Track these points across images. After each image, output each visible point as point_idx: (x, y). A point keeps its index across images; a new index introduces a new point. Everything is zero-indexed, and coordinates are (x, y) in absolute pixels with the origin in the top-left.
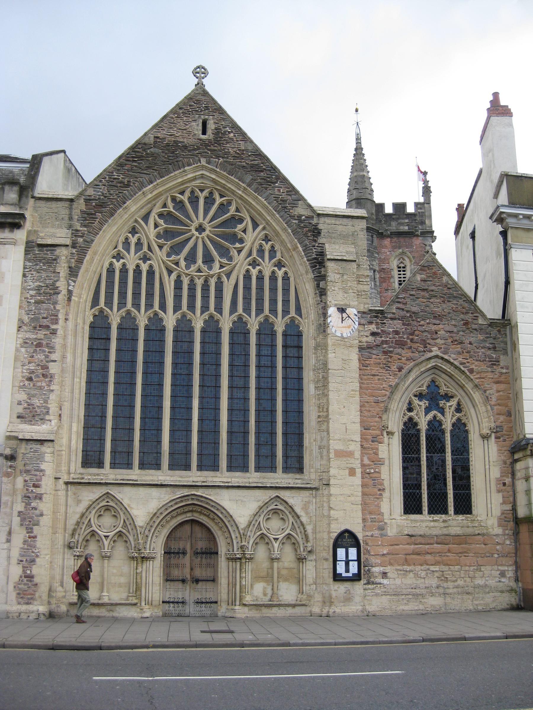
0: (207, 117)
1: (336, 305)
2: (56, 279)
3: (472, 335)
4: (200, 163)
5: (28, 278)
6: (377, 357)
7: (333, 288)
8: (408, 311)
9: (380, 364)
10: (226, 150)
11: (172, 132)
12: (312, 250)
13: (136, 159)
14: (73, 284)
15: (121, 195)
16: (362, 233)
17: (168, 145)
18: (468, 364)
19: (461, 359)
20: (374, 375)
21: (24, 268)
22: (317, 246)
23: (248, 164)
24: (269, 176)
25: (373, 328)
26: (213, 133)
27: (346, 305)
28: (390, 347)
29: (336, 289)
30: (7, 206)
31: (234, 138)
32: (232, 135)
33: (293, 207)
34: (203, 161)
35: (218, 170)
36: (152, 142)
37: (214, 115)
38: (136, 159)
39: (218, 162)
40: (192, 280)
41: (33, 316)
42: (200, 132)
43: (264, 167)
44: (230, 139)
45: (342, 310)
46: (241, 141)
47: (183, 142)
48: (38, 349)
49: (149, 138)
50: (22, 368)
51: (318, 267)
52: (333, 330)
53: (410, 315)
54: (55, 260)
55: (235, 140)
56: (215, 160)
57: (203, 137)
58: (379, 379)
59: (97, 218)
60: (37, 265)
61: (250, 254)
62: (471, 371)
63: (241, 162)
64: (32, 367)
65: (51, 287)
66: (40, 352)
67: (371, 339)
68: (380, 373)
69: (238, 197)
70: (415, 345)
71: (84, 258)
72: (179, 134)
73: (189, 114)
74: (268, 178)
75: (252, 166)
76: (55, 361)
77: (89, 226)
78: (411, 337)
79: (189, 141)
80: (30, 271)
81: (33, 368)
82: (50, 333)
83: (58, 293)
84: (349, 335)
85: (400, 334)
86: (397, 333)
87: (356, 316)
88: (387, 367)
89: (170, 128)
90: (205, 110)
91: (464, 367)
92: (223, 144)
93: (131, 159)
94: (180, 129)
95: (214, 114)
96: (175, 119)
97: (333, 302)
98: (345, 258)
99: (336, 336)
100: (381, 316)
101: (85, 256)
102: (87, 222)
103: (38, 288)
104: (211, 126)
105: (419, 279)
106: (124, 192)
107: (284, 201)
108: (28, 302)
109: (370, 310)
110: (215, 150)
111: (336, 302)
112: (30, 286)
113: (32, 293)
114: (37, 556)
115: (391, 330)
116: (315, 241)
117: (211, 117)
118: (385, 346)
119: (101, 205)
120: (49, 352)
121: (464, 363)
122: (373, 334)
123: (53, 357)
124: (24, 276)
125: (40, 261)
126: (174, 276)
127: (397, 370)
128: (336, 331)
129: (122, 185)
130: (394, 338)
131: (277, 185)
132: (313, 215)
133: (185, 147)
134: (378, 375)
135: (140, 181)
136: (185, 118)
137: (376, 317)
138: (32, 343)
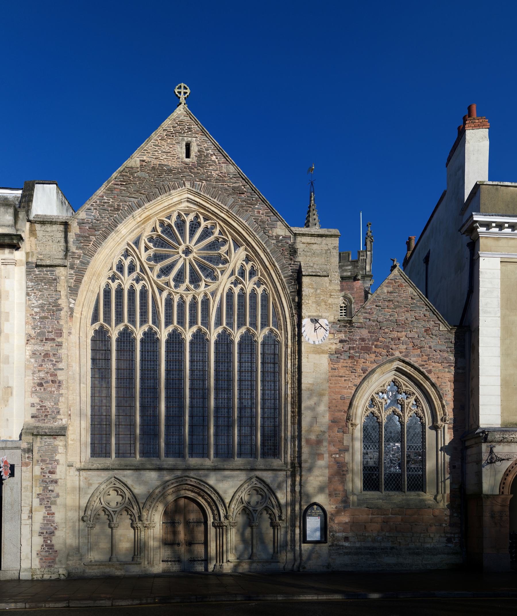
0: (190, 139)
1: (309, 317)
2: (57, 297)
3: (432, 340)
4: (185, 186)
5: (32, 297)
6: (344, 362)
7: (307, 302)
8: (373, 321)
9: (347, 367)
10: (209, 173)
11: (157, 155)
12: (288, 267)
13: (124, 183)
14: (73, 302)
15: (112, 218)
16: (334, 251)
17: (153, 168)
18: (426, 366)
19: (421, 362)
20: (341, 377)
21: (27, 288)
22: (293, 264)
23: (228, 186)
24: (249, 198)
25: (342, 336)
26: (196, 156)
27: (319, 316)
28: (356, 352)
29: (310, 302)
30: (4, 227)
31: (217, 160)
32: (214, 158)
33: (271, 228)
34: (188, 185)
35: (202, 193)
36: (138, 166)
37: (197, 137)
38: (124, 183)
39: (202, 185)
40: (182, 297)
41: (39, 331)
42: (184, 155)
43: (245, 189)
44: (213, 161)
45: (315, 321)
46: (223, 163)
47: (168, 165)
48: (46, 359)
49: (135, 162)
50: (33, 376)
51: (293, 283)
52: (307, 339)
53: (376, 324)
54: (55, 279)
55: (217, 162)
56: (198, 183)
57: (187, 160)
58: (345, 380)
59: (91, 241)
60: (38, 284)
61: (233, 273)
62: (430, 372)
63: (223, 185)
64: (42, 375)
65: (53, 304)
66: (48, 361)
67: (339, 346)
68: (347, 374)
69: (220, 220)
70: (377, 350)
71: (82, 278)
72: (164, 157)
73: (173, 136)
74: (249, 200)
75: (234, 188)
76: (63, 369)
77: (84, 248)
78: (375, 343)
79: (173, 164)
80: (33, 290)
81: (43, 376)
82: (56, 345)
83: (61, 310)
84: (320, 342)
85: (366, 341)
86: (363, 340)
87: (327, 325)
88: (353, 371)
89: (155, 151)
90: (188, 132)
91: (422, 368)
92: (205, 166)
93: (119, 183)
94: (164, 152)
95: (197, 136)
96: (159, 141)
97: (307, 314)
98: (319, 274)
99: (309, 344)
100: (349, 325)
101: (83, 276)
102: (82, 244)
103: (42, 307)
104: (194, 149)
105: (386, 291)
106: (115, 215)
107: (263, 222)
108: (33, 318)
109: (339, 321)
110: (198, 173)
111: (310, 314)
112: (34, 304)
113: (36, 310)
114: (56, 529)
115: (358, 338)
116: (291, 259)
117: (194, 139)
118: (352, 351)
119: (94, 228)
120: (56, 362)
121: (423, 365)
122: (341, 341)
123: (60, 366)
124: (28, 294)
125: (41, 281)
126: (165, 294)
127: (362, 372)
128: (309, 339)
129: (112, 208)
130: (360, 344)
131: (256, 206)
132: (291, 235)
133: (170, 171)
134: (345, 377)
135: (129, 205)
136: (169, 141)
137: (345, 326)
138: (40, 354)
